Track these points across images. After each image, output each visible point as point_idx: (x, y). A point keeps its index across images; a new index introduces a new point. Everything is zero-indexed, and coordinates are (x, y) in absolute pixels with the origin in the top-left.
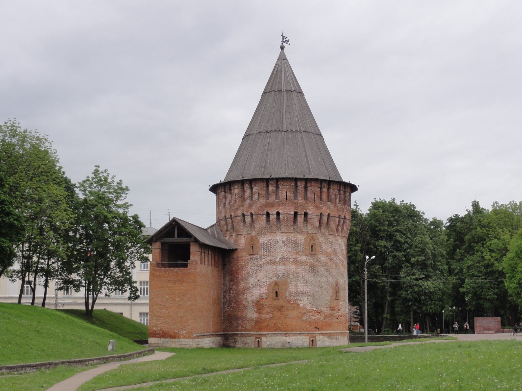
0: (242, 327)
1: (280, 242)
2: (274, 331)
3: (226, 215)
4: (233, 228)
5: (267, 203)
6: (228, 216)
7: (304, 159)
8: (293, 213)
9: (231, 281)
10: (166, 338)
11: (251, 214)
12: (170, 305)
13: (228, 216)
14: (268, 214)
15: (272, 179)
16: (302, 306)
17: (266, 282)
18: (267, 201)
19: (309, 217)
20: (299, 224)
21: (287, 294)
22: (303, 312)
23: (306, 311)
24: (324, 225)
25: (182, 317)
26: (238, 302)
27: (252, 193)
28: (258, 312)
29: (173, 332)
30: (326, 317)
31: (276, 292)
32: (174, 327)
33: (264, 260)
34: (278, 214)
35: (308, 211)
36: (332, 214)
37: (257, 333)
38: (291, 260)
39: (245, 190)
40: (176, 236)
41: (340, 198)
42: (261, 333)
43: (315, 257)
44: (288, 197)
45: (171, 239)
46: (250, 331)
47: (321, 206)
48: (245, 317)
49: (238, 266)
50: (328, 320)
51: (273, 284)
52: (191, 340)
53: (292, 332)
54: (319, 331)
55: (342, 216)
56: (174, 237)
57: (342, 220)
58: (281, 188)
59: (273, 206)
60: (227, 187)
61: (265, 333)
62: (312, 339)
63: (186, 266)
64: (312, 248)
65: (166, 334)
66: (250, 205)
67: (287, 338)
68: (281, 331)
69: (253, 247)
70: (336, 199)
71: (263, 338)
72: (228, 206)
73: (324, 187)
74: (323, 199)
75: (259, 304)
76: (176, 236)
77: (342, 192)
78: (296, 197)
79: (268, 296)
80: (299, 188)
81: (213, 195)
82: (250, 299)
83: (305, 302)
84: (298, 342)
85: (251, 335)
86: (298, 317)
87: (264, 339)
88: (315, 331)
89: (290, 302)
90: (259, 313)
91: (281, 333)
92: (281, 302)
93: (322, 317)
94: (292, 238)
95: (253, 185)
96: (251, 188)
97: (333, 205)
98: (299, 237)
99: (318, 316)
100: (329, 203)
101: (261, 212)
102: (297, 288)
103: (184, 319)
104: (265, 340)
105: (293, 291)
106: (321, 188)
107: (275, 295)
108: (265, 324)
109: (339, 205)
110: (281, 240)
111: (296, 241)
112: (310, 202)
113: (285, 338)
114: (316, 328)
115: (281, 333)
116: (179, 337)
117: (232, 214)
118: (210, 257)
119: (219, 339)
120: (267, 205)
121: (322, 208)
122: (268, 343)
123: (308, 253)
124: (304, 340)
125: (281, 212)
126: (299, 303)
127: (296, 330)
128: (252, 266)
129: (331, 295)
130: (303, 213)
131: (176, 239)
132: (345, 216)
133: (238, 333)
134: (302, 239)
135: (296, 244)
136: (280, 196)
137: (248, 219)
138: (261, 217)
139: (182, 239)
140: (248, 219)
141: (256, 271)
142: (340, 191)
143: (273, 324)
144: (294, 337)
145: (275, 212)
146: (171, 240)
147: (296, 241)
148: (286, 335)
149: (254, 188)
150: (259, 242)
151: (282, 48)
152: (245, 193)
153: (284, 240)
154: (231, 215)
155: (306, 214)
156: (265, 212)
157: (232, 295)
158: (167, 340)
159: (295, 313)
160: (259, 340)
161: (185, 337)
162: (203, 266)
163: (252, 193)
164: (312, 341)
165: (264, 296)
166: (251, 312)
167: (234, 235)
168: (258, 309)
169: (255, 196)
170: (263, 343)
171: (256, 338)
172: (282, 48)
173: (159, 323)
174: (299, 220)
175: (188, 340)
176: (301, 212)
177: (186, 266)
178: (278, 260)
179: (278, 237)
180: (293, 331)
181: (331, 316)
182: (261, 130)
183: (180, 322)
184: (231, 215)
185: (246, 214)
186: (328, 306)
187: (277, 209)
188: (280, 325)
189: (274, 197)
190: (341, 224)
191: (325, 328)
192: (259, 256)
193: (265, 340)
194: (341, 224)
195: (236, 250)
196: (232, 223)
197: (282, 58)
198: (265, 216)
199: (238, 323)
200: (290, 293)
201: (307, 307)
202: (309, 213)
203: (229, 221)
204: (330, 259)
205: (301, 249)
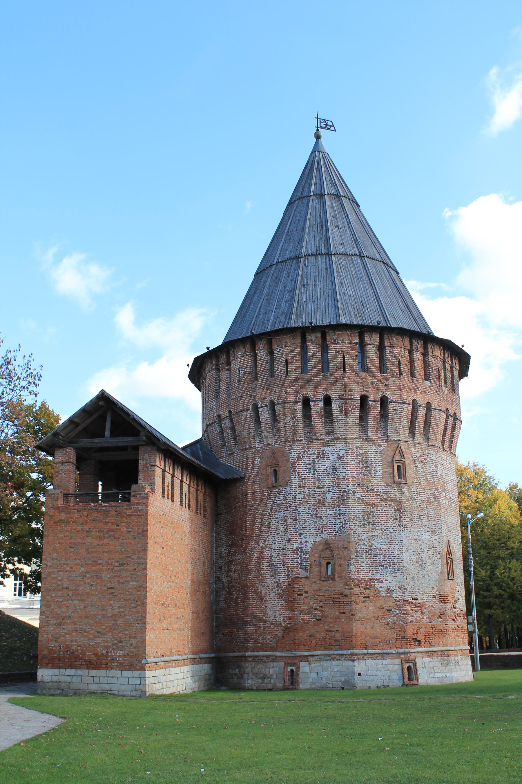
0: (256, 641)
1: (333, 457)
2: (326, 649)
4: (235, 438)
5: (303, 379)
6: (224, 414)
7: (372, 299)
8: (358, 396)
9: (232, 545)
10: (76, 668)
11: (273, 404)
12: (88, 590)
13: (224, 414)
14: (306, 402)
15: (314, 329)
17: (306, 542)
18: (304, 375)
19: (391, 406)
21: (352, 568)
22: (386, 606)
24: (420, 427)
25: (115, 617)
26: (246, 589)
27: (272, 362)
28: (291, 606)
29: (96, 654)
33: (299, 496)
34: (327, 401)
35: (388, 394)
36: (434, 405)
38: (358, 495)
39: (258, 358)
40: (107, 433)
42: (299, 654)
45: (96, 440)
46: (273, 649)
47: (413, 385)
48: (261, 619)
49: (245, 513)
50: (436, 622)
51: (320, 548)
52: (136, 673)
53: (365, 651)
56: (103, 436)
57: (451, 419)
58: (331, 347)
59: (316, 385)
60: (223, 358)
61: (306, 653)
63: (126, 499)
65: (77, 658)
66: (269, 387)
68: (341, 648)
69: (277, 473)
71: (301, 664)
72: (223, 396)
74: (417, 373)
76: (107, 433)
79: (311, 573)
80: (368, 348)
82: (271, 582)
84: (379, 673)
85: (275, 659)
87: (304, 667)
90: (292, 610)
91: (340, 652)
92: (339, 586)
95: (274, 346)
96: (271, 353)
97: (435, 388)
98: (373, 447)
100: (428, 383)
101: (291, 398)
103: (120, 621)
105: (364, 560)
108: (303, 635)
112: (392, 376)
114: (415, 640)
115: (340, 652)
116: (107, 667)
120: (303, 384)
121: (415, 390)
122: (313, 675)
123: (390, 481)
124: (391, 667)
125: (333, 395)
126: (378, 586)
127: (375, 646)
128: (275, 511)
129: (439, 570)
130: (379, 398)
131: (108, 439)
133: (248, 654)
136: (331, 365)
137: (265, 415)
138: (292, 407)
139: (121, 439)
140: (265, 415)
141: (284, 521)
143: (323, 634)
144: (370, 662)
145: (321, 396)
146: (97, 442)
149: (277, 351)
150: (288, 461)
151: (318, 137)
152: (259, 363)
153: (342, 453)
154: (230, 412)
155: (384, 401)
157: (234, 575)
158: (80, 672)
160: (294, 668)
161: (121, 667)
162: (167, 502)
163: (272, 362)
164: (409, 668)
165: (302, 573)
167: (236, 451)
168: (289, 602)
169: (280, 367)
170: (301, 675)
171: (287, 664)
172: (318, 137)
173: (62, 632)
176: (374, 396)
178: (329, 496)
179: (327, 449)
180: (366, 649)
181: (442, 614)
182: (286, 257)
183: (111, 630)
184: (230, 412)
186: (435, 592)
188: (338, 636)
190: (449, 427)
191: (432, 639)
192: (288, 488)
193: (307, 669)
194: (449, 427)
195: (242, 479)
196: (233, 428)
199: (246, 633)
200: (359, 565)
202: (391, 398)
203: (226, 423)
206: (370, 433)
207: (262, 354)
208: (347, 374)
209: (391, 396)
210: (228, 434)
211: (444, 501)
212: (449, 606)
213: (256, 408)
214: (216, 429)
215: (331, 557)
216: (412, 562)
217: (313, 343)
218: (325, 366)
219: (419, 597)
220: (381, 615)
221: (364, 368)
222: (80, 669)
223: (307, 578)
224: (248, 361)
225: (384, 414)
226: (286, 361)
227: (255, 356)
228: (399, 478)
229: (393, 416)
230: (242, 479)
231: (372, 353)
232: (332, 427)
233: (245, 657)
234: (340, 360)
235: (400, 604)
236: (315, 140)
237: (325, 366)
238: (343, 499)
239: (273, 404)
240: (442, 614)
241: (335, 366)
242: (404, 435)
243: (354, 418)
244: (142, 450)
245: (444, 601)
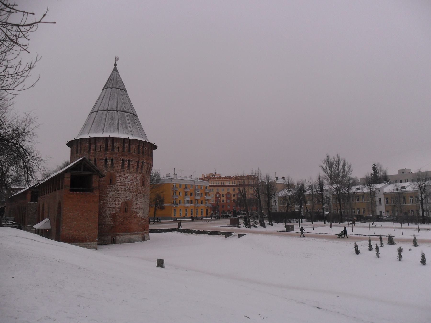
1: (129, 178)
14: (123, 161)
17: (120, 202)
19: (144, 164)
31: (126, 208)
32: (83, 234)
33: (119, 188)
34: (129, 161)
68: (128, 232)
69: (112, 181)
75: (114, 216)
85: (108, 235)
87: (118, 237)
101: (119, 159)
102: (136, 206)
104: (119, 238)
110: (130, 176)
111: (137, 178)
113: (130, 236)
117: (96, 158)
125: (131, 160)
126: (137, 214)
134: (139, 176)
135: (137, 179)
137: (109, 162)
140: (109, 162)
147: (137, 178)
148: (131, 235)
153: (131, 176)
161: (90, 241)
165: (118, 211)
169: (116, 149)
175: (92, 243)
178: (127, 189)
179: (127, 175)
193: (119, 238)
205: (139, 182)
213: (106, 160)
217: (127, 143)
224: (104, 144)
225: (142, 166)
226: (118, 147)
236: (114, 66)
237: (129, 151)
239: (112, 160)
241: (132, 151)
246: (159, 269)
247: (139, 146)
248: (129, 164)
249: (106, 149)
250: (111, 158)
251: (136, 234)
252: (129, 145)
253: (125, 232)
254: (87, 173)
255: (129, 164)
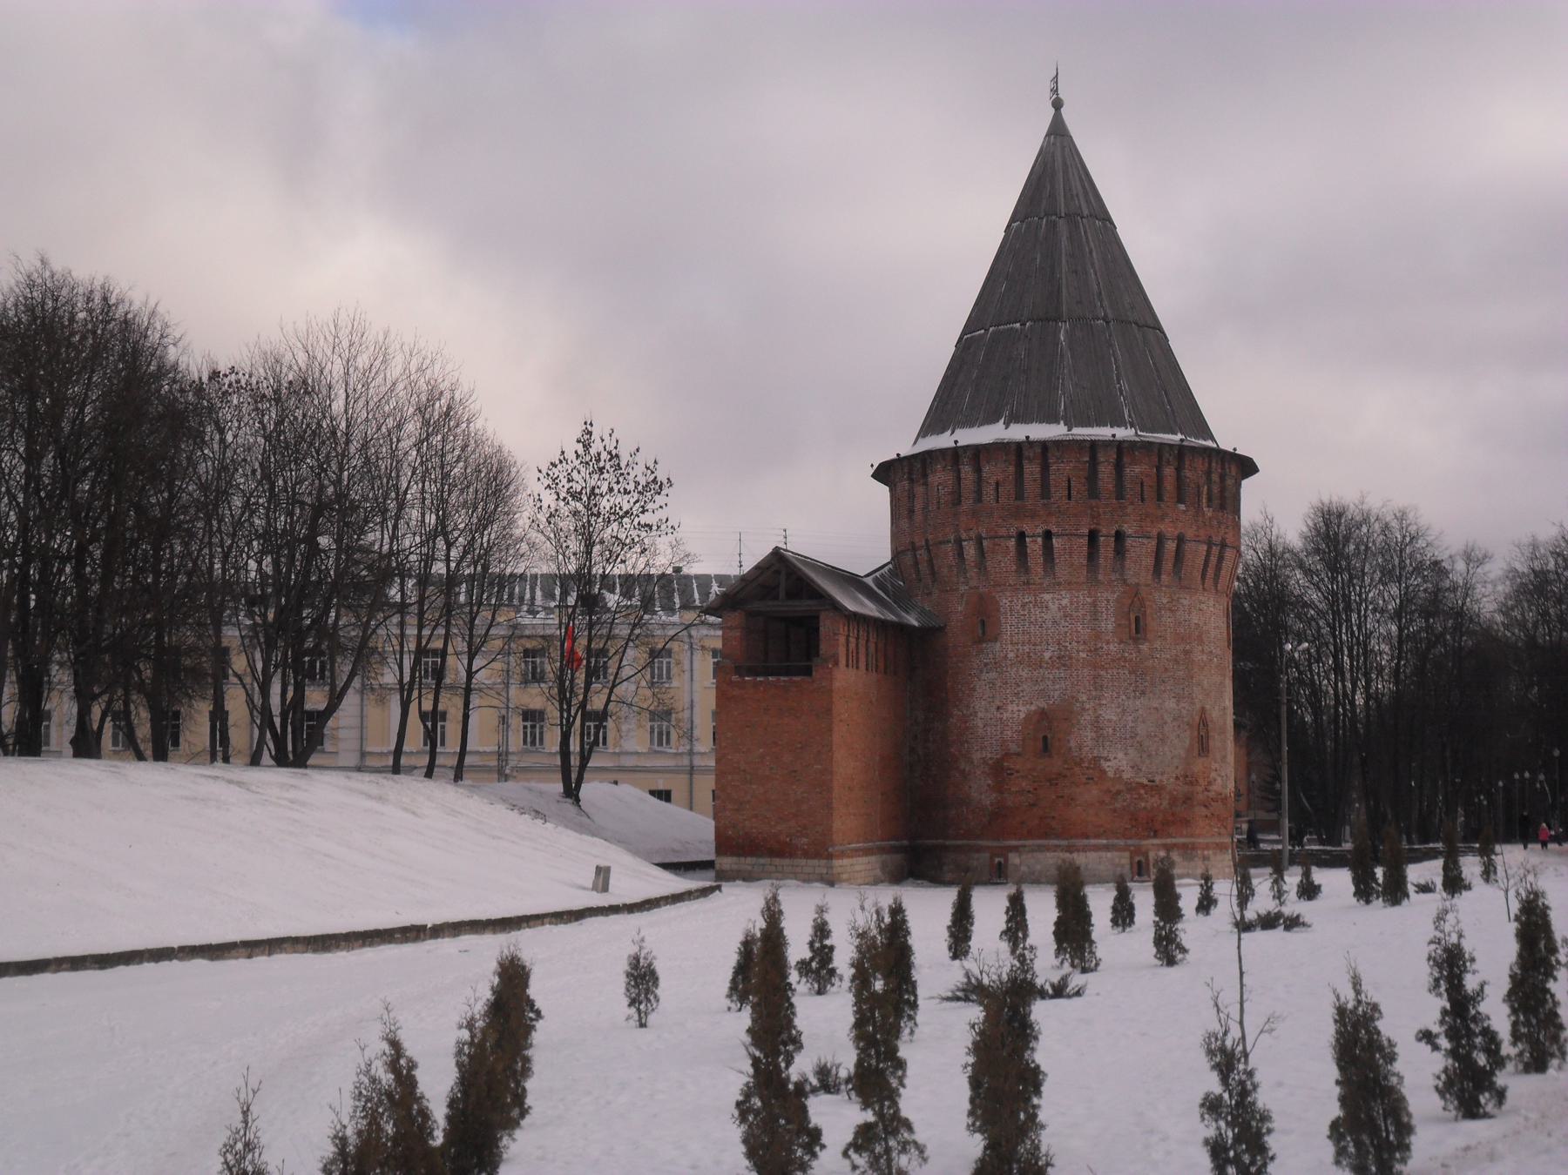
1: (1053, 607)
2: (1040, 838)
3: (916, 540)
4: (933, 573)
6: (920, 542)
14: (1021, 536)
16: (1111, 774)
17: (1018, 711)
19: (1129, 542)
20: (1101, 561)
21: (1073, 744)
22: (1114, 790)
23: (1121, 787)
24: (1168, 565)
27: (979, 481)
30: (1174, 801)
31: (1045, 738)
33: (1011, 655)
34: (1048, 535)
36: (1189, 534)
37: (995, 844)
38: (1083, 655)
41: (1209, 490)
43: (1144, 647)
44: (1074, 493)
47: (1159, 513)
52: (823, 862)
54: (1155, 836)
55: (1217, 539)
59: (1033, 515)
62: (1137, 859)
63: (807, 672)
64: (1137, 627)
67: (1075, 855)
68: (1058, 836)
69: (985, 624)
70: (1199, 495)
71: (1011, 855)
72: (918, 517)
73: (1168, 462)
75: (999, 771)
77: (1215, 477)
78: (1093, 492)
80: (1101, 468)
81: (883, 492)
82: (976, 756)
83: (1118, 762)
85: (979, 850)
86: (1102, 803)
87: (1014, 859)
88: (1148, 837)
89: (1079, 764)
91: (1056, 842)
93: (1165, 803)
94: (1084, 598)
99: (1153, 801)
100: (1182, 507)
101: (1002, 532)
102: (1097, 725)
105: (1089, 734)
106: (1159, 469)
107: (1040, 744)
109: (1209, 512)
110: (1056, 602)
111: (1094, 604)
113: (1067, 855)
116: (792, 855)
118: (872, 647)
119: (898, 857)
122: (1024, 868)
125: (1054, 530)
126: (1105, 765)
127: (1097, 836)
132: (1224, 539)
134: (1108, 598)
135: (1096, 613)
137: (970, 551)
140: (970, 551)
142: (1209, 473)
144: (1092, 855)
145: (1039, 531)
147: (1094, 604)
148: (1070, 849)
153: (1065, 602)
156: (1013, 531)
158: (762, 861)
159: (1094, 792)
161: (807, 855)
162: (852, 672)
163: (979, 481)
164: (1139, 863)
165: (1013, 748)
166: (980, 791)
169: (989, 492)
174: (1102, 550)
175: (816, 862)
176: (1107, 531)
177: (807, 672)
178: (1047, 655)
179: (1047, 597)
181: (1188, 799)
185: (964, 536)
187: (1045, 522)
189: (1038, 491)
190: (1214, 560)
193: (1017, 861)
194: (1214, 560)
195: (941, 629)
196: (930, 561)
197: (1058, 130)
198: (1012, 543)
200: (1083, 739)
201: (1125, 776)
203: (922, 554)
204: (1186, 652)
205: (1108, 625)
206: (1100, 577)
207: (967, 470)
208: (1073, 502)
209: (1128, 529)
210: (924, 567)
211: (1198, 656)
212: (1200, 789)
213: (959, 541)
214: (908, 559)
215: (1047, 731)
216: (1149, 736)
218: (1045, 492)
219: (1157, 779)
220: (1107, 800)
221: (1093, 492)
222: (761, 856)
223: (1018, 754)
227: (959, 471)
228: (1137, 631)
229: (1131, 554)
230: (941, 629)
231: (1106, 471)
232: (1053, 568)
233: (946, 848)
234: (1065, 484)
235: (1132, 787)
237: (1045, 492)
238: (1063, 660)
239: (979, 540)
240: (1188, 799)
241: (1058, 493)
242: (1145, 577)
243: (1081, 559)
244: (823, 616)
245: (1191, 783)
246: (603, 864)
247: (1094, 463)
248: (1048, 549)
249: (957, 500)
250: (973, 534)
251: (1096, 848)
252: (1045, 468)
253: (1045, 836)
254: (803, 606)
255: (1048, 549)
